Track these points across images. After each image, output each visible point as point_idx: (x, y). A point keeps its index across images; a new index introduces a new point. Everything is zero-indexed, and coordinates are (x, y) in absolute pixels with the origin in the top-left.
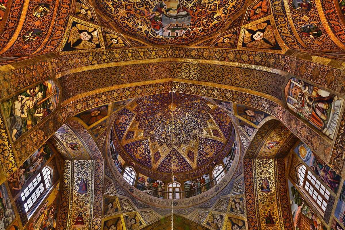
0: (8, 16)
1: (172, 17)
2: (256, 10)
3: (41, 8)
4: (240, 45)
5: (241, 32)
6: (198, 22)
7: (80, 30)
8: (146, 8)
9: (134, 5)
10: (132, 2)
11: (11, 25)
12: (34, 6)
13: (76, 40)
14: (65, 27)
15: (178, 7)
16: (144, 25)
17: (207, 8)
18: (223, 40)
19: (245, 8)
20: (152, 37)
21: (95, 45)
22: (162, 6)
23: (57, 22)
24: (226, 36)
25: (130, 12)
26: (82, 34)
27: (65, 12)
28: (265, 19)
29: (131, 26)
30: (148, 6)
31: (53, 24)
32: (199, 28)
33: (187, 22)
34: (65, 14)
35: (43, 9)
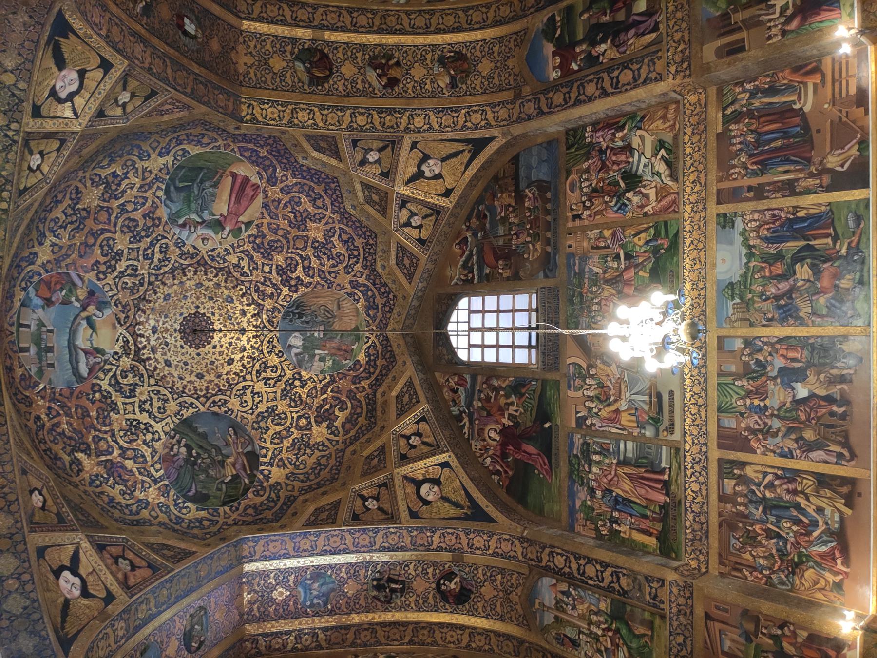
1: (73, 333)
2: (125, 559)
4: (38, 539)
5: (68, 534)
6: (62, 407)
7: (87, 75)
8: (97, 262)
9: (109, 231)
10: (115, 226)
13: (66, 56)
14: (107, 39)
15: (99, 351)
16: (54, 253)
17: (100, 431)
18: (36, 489)
19: (120, 531)
20: (19, 274)
21: (39, 104)
22: (102, 306)
23: (117, 21)
24: (47, 496)
25: (92, 217)
26: (74, 75)
28: (115, 588)
29: (53, 215)
30: (103, 268)
32: (47, 415)
33: (59, 377)
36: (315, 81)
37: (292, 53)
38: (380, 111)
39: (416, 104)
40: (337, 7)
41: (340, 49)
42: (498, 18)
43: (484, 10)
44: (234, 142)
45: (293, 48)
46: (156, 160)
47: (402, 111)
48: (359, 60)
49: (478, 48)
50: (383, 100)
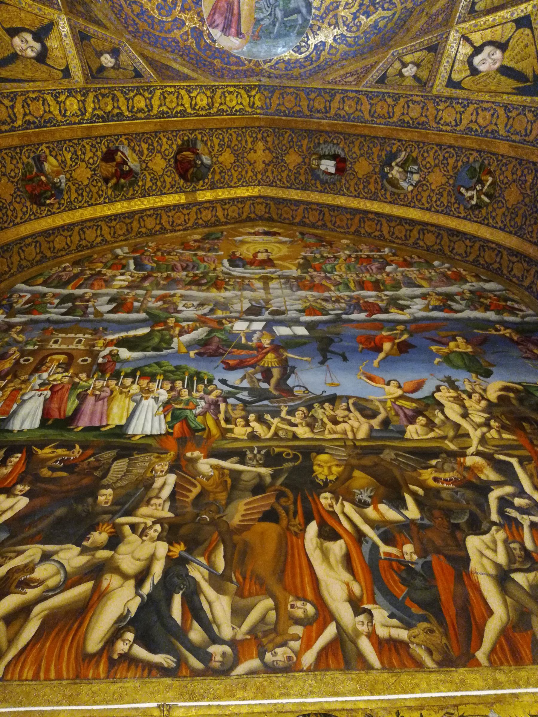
0: (404, 247)
3: (394, 172)
7: (468, 72)
11: (430, 239)
12: (386, 190)
13: (503, 78)
21: (521, 30)
23: (444, 128)
26: (482, 68)
27: (418, 108)
31: (448, 140)
34: (423, 108)
35: (396, 168)
36: (189, 146)
37: (214, 172)
38: (120, 116)
39: (79, 131)
40: (175, 231)
41: (168, 186)
42: (7, 255)
43: (24, 263)
44: (253, 70)
45: (213, 178)
46: (327, 37)
47: (95, 118)
48: (149, 178)
49: (20, 214)
50: (118, 131)
